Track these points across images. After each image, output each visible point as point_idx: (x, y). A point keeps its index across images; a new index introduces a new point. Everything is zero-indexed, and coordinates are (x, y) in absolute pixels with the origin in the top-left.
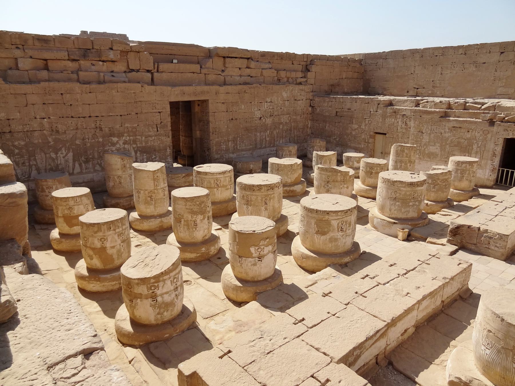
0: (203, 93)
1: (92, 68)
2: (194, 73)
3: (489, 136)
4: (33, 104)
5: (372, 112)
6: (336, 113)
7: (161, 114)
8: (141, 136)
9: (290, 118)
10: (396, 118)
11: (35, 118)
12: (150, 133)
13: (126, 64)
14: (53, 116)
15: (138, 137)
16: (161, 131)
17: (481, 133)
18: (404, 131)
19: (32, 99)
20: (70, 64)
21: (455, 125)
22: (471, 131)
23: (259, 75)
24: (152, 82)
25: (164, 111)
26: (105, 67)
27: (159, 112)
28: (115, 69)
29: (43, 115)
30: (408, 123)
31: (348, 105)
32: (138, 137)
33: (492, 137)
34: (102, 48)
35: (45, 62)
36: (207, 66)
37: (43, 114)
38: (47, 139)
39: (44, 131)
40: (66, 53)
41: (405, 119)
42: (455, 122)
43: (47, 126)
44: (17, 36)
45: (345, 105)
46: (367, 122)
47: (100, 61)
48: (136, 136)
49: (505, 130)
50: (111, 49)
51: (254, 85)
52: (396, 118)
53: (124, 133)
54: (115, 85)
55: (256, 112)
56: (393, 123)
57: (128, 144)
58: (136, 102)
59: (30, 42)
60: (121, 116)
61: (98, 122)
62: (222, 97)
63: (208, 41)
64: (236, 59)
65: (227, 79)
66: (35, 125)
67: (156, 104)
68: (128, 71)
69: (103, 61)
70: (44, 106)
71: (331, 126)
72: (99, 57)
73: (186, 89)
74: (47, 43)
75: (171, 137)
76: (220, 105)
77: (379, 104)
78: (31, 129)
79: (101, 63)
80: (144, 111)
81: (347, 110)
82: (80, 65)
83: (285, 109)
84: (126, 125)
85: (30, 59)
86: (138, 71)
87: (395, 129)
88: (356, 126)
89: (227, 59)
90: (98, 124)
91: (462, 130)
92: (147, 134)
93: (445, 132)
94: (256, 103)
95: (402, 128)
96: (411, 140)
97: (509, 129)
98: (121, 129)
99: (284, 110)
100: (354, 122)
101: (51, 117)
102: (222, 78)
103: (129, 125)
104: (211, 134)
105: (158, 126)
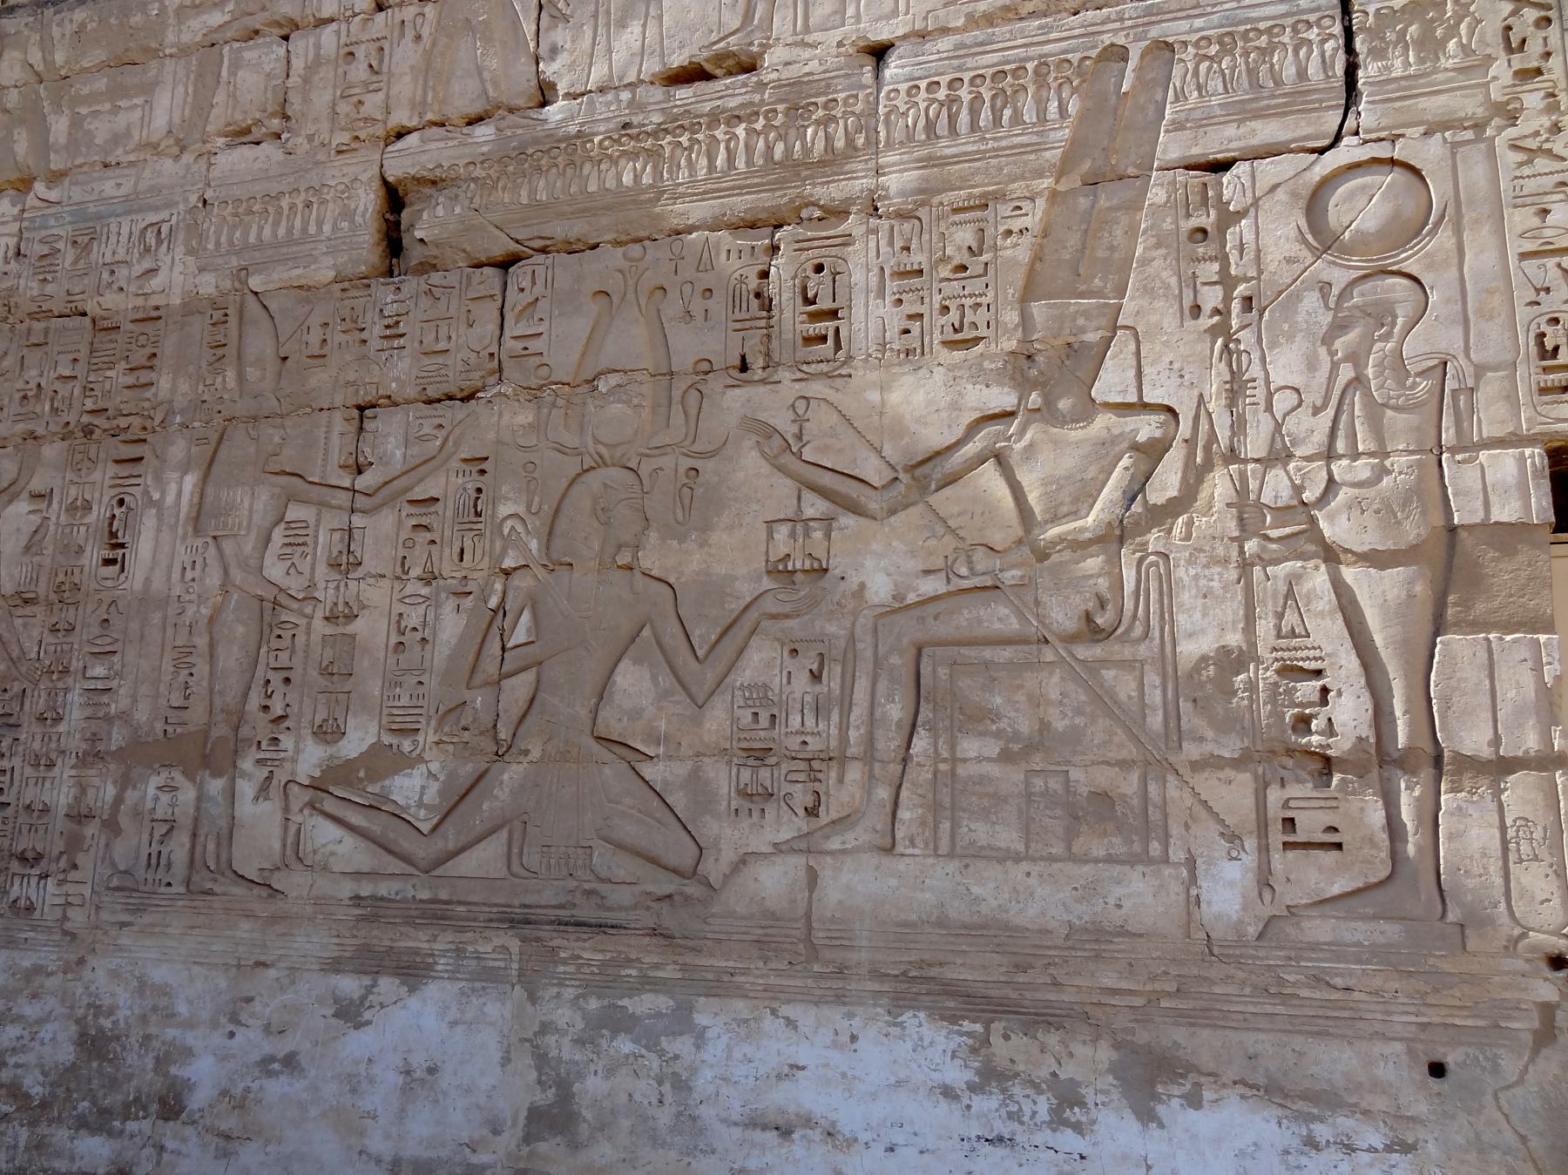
6: (393, 242)
100: (871, 317)
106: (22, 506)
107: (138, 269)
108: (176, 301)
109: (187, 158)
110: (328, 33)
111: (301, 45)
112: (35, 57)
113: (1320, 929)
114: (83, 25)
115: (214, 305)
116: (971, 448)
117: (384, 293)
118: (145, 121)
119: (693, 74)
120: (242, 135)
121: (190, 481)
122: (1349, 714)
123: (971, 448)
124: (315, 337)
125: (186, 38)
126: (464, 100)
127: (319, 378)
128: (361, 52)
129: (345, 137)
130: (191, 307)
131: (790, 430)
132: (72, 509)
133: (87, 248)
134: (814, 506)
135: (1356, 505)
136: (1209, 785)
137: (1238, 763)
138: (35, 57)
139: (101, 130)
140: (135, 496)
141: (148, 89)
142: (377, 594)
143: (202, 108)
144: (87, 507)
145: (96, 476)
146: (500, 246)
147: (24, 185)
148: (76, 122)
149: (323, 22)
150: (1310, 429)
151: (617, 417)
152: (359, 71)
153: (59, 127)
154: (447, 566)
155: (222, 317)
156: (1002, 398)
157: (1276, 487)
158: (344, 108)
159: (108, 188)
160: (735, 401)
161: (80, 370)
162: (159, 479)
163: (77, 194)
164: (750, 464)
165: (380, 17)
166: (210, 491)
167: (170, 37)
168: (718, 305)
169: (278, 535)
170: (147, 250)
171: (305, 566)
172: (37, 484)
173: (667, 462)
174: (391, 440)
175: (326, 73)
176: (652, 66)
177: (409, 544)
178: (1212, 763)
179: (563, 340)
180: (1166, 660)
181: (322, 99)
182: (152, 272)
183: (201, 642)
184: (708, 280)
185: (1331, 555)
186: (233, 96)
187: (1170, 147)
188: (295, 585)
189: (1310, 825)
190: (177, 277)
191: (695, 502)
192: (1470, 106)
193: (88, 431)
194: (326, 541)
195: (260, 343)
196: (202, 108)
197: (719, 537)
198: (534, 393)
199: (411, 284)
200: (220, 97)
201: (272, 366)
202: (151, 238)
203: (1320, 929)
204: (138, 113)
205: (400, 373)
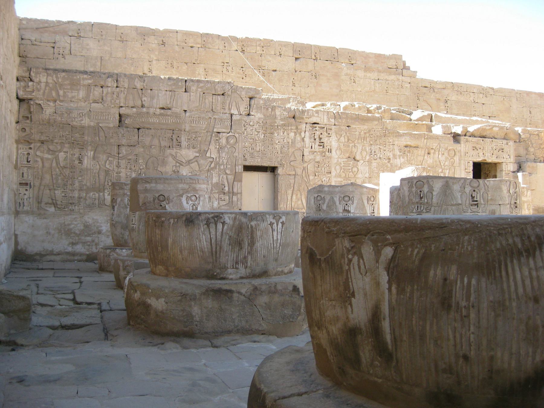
3: (456, 158)
5: (234, 118)
10: (298, 131)
17: (446, 154)
18: (318, 158)
21: (409, 143)
22: (432, 151)
30: (325, 140)
31: (162, 99)
33: (460, 160)
41: (318, 133)
42: (408, 138)
45: (152, 98)
46: (224, 141)
49: (475, 148)
52: (298, 131)
56: (293, 142)
71: (103, 157)
77: (251, 98)
81: (158, 111)
87: (298, 154)
88: (191, 154)
91: (421, 152)
93: (395, 156)
95: (313, 152)
96: (335, 176)
97: (478, 146)
100: (184, 143)
106: (62, 153)
107: (79, 119)
108: (87, 125)
109: (86, 103)
110: (109, 89)
111: (105, 90)
112: (55, 79)
113: (223, 207)
114: (64, 76)
115: (93, 127)
116: (194, 160)
117: (121, 130)
118: (78, 95)
119: (163, 108)
120: (95, 102)
121: (92, 153)
122: (227, 189)
123: (194, 160)
124: (111, 134)
125: (84, 83)
126: (131, 104)
127: (112, 141)
128: (115, 93)
129: (112, 106)
130: (89, 127)
131: (175, 155)
132: (72, 155)
133: (69, 114)
134: (178, 164)
135: (229, 169)
136: (215, 195)
137: (217, 193)
138: (55, 79)
139: (70, 95)
140: (83, 154)
141: (78, 90)
142: (123, 171)
143: (88, 95)
144: (75, 155)
145: (76, 150)
146: (138, 127)
147: (55, 101)
148: (65, 93)
149: (107, 87)
150: (225, 161)
151: (154, 151)
152: (115, 96)
153: (61, 93)
154: (133, 168)
155: (97, 130)
156: (198, 155)
157: (222, 167)
158: (112, 101)
159: (72, 105)
160: (168, 151)
161: (70, 133)
162: (87, 152)
163: (66, 105)
164: (170, 159)
165: (118, 89)
166: (96, 155)
167: (82, 82)
168: (166, 139)
169: (108, 161)
170: (81, 117)
171: (112, 166)
172: (65, 150)
173: (161, 157)
174: (124, 150)
175: (109, 95)
176: (158, 106)
177: (127, 164)
178: (215, 193)
179: (147, 140)
180: (212, 183)
181: (109, 99)
182: (82, 120)
183: (97, 175)
184: (165, 136)
185: (226, 174)
186: (93, 95)
187: (215, 130)
188: (111, 168)
189: (223, 198)
190: (86, 122)
191: (164, 163)
192: (241, 132)
193: (73, 143)
194: (115, 163)
195: (102, 134)
196: (88, 95)
197: (167, 167)
198: (143, 147)
199: (125, 129)
200: (91, 94)
201: (104, 138)
202: (81, 115)
203: (223, 207)
204: (76, 94)
205: (124, 142)
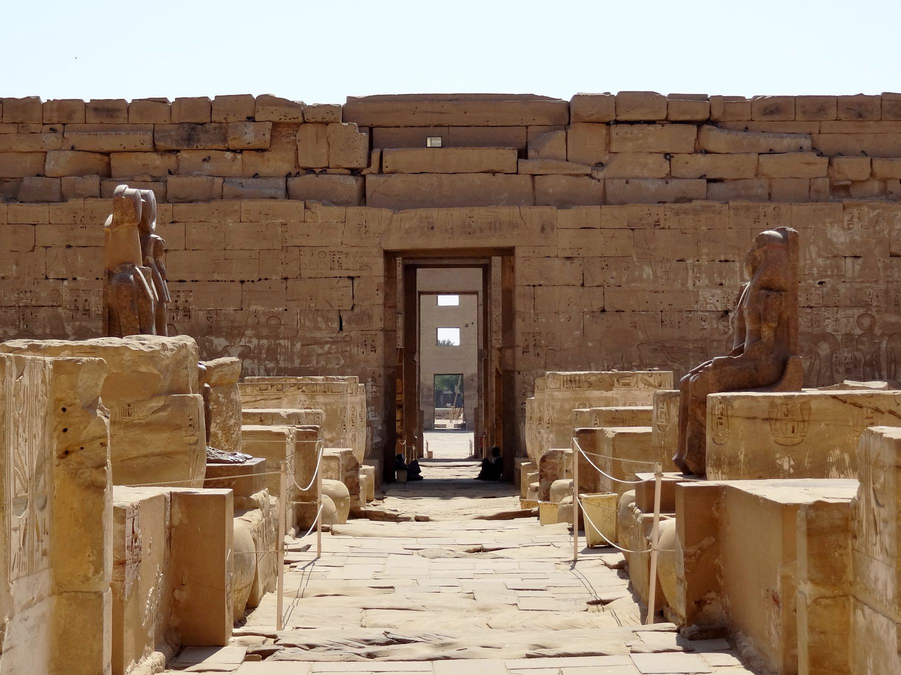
0: (494, 226)
1: (198, 167)
2: (494, 173)
4: (46, 247)
7: (356, 282)
8: (292, 339)
9: (866, 322)
11: (47, 278)
12: (318, 335)
13: (291, 155)
14: (83, 275)
15: (282, 342)
16: (352, 331)
19: (48, 235)
20: (156, 160)
23: (750, 174)
24: (363, 198)
25: (364, 274)
26: (228, 162)
27: (352, 278)
28: (264, 170)
29: (63, 271)
32: (282, 342)
34: (231, 119)
35: (106, 158)
36: (546, 150)
37: (63, 269)
38: (64, 328)
39: (60, 309)
40: (148, 137)
43: (66, 297)
44: (55, 106)
47: (228, 150)
48: (277, 337)
50: (251, 119)
51: (696, 203)
53: (246, 327)
54: (236, 204)
55: (705, 294)
57: (253, 359)
58: (285, 249)
59: (79, 116)
60: (242, 282)
61: (182, 294)
62: (564, 241)
63: (560, 81)
64: (651, 128)
65: (610, 188)
66: (43, 294)
67: (343, 256)
68: (294, 172)
69: (234, 151)
70: (69, 252)
72: (225, 140)
73: (438, 215)
74: (112, 116)
75: (380, 350)
76: (557, 263)
78: (33, 303)
79: (229, 155)
80: (306, 273)
82: (178, 161)
83: (842, 288)
84: (253, 308)
85: (70, 154)
86: (324, 170)
89: (614, 129)
90: (182, 299)
92: (308, 335)
94: (704, 261)
98: (239, 316)
99: (835, 290)
101: (79, 278)
102: (600, 185)
103: (260, 308)
104: (519, 351)
105: (345, 317)
